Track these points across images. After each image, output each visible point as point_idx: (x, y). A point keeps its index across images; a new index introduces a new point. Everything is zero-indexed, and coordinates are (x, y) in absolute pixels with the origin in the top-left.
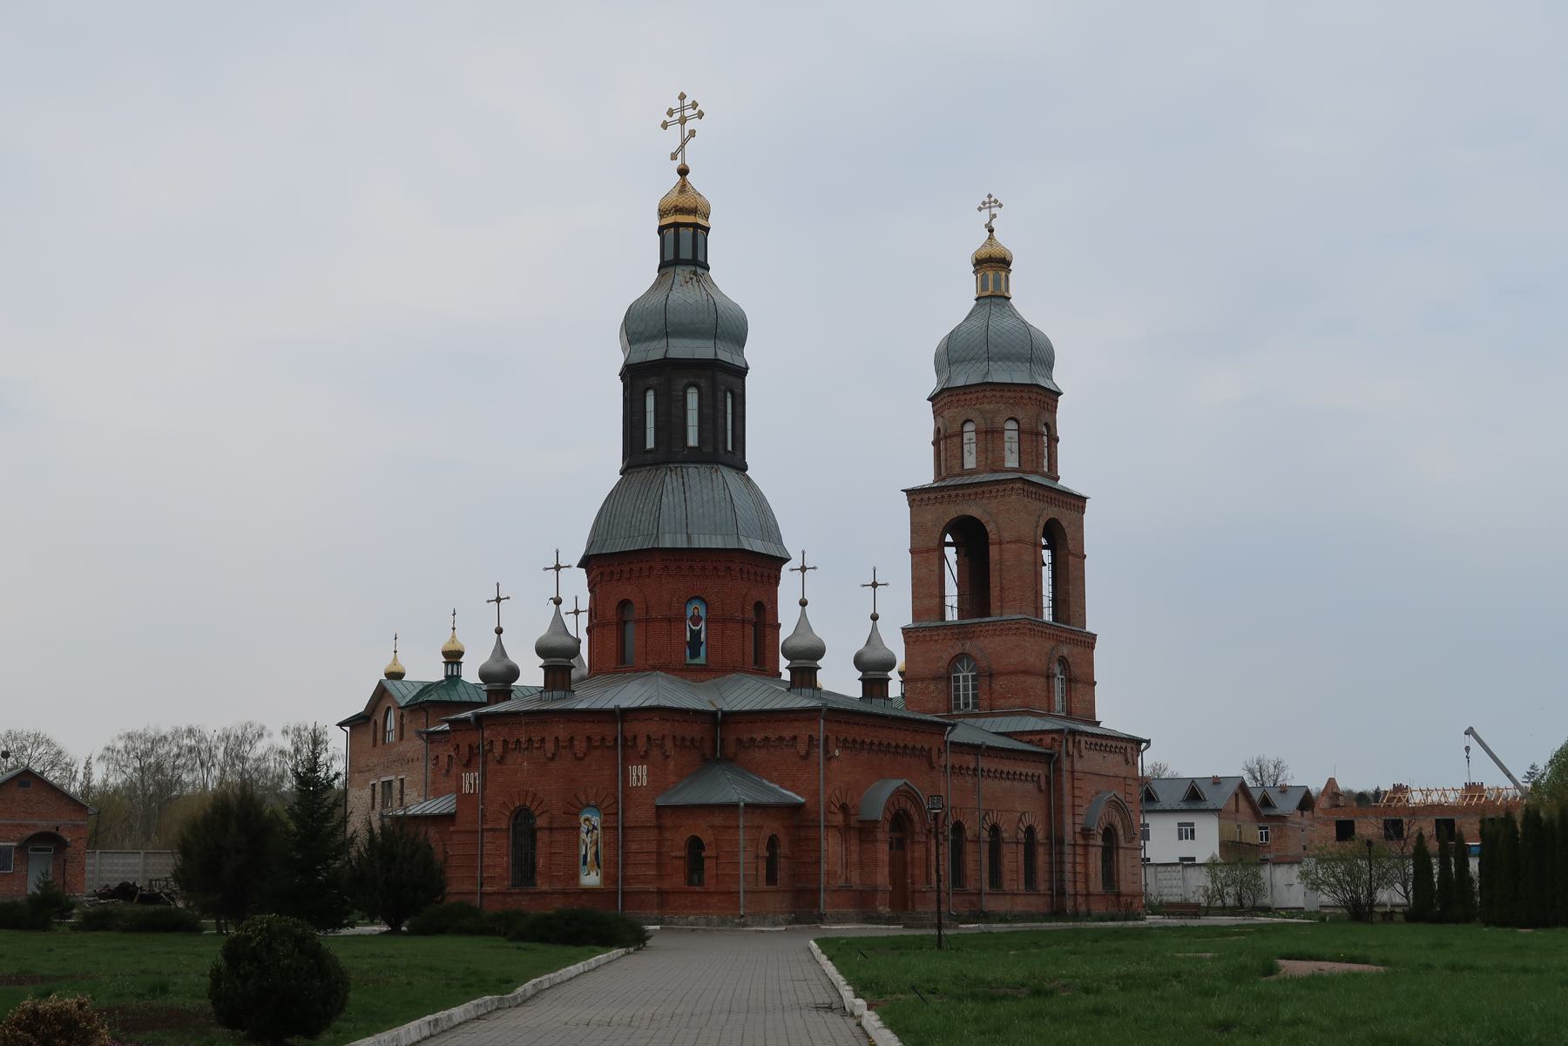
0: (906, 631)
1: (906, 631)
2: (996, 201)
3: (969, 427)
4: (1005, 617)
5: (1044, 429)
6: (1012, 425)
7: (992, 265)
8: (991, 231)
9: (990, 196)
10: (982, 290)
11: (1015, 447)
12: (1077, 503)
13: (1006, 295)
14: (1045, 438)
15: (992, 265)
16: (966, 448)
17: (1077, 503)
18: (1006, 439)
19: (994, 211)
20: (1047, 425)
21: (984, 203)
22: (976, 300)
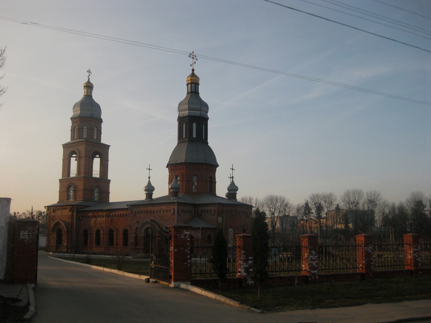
0: (60, 180)
1: (60, 180)
2: (90, 72)
3: (76, 128)
4: (80, 176)
5: (96, 128)
6: (85, 127)
7: (89, 86)
8: (89, 79)
9: (89, 70)
10: (84, 94)
11: (86, 133)
12: (107, 147)
13: (91, 95)
14: (95, 131)
15: (89, 86)
16: (75, 133)
17: (107, 147)
18: (84, 131)
19: (90, 74)
20: (96, 127)
21: (88, 71)
22: (84, 95)
